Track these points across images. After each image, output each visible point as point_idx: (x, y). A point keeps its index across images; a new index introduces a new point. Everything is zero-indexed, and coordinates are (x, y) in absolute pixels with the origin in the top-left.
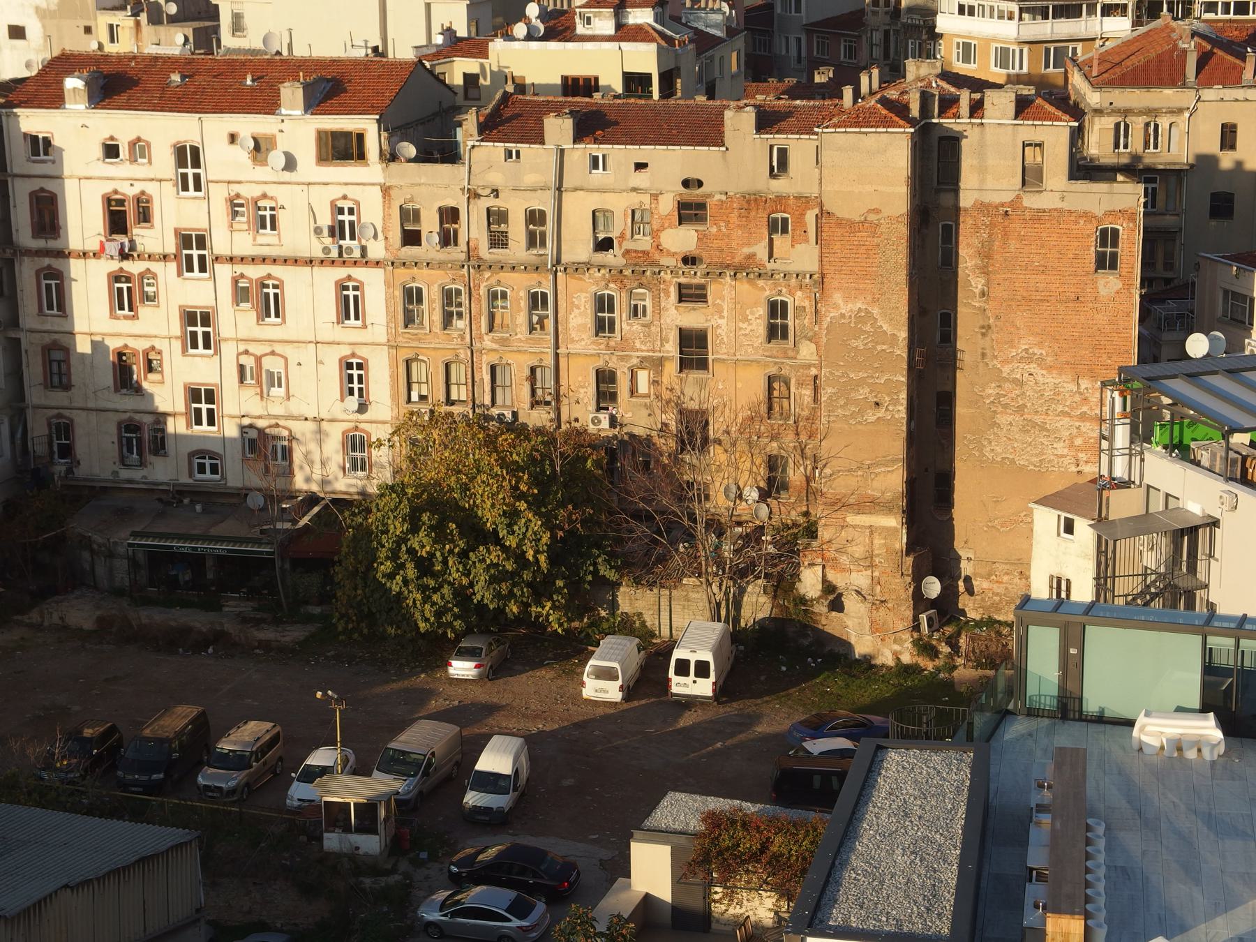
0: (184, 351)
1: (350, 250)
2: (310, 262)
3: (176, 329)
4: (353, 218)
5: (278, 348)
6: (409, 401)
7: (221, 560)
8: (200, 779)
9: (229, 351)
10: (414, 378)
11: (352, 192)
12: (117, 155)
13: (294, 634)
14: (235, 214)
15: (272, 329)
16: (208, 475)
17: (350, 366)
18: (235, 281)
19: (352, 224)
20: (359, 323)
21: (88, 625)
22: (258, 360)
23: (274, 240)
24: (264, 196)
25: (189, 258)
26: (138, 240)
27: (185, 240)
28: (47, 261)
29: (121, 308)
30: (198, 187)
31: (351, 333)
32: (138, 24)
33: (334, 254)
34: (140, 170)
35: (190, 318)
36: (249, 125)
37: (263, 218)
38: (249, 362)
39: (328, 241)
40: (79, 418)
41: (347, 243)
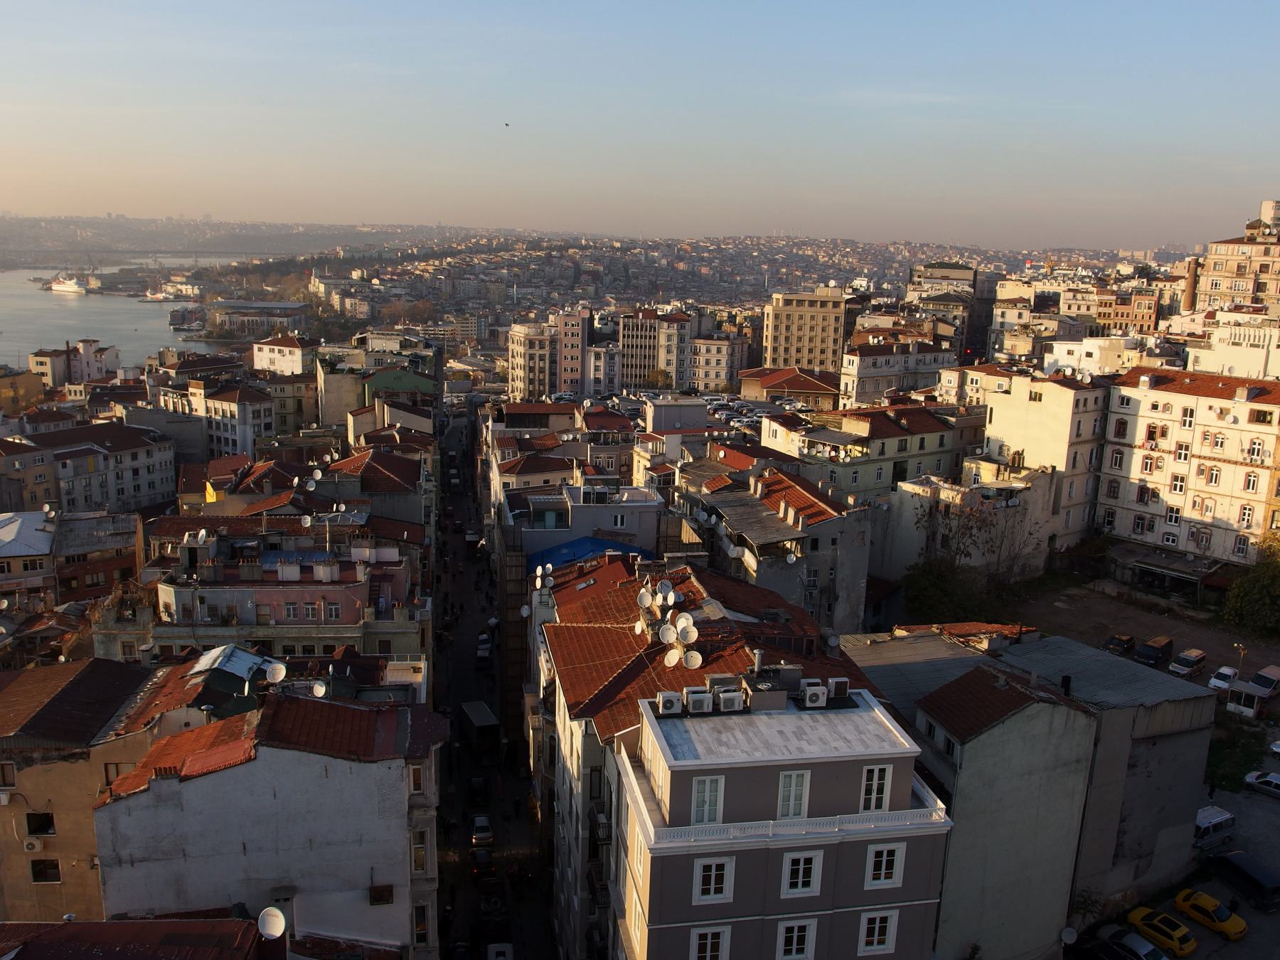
0: (1170, 491)
1: (1256, 460)
2: (1236, 463)
3: (1168, 482)
4: (1260, 447)
5: (1213, 496)
6: (1271, 528)
7: (1173, 578)
8: (1170, 667)
9: (1190, 494)
10: (1276, 519)
11: (1262, 436)
12: (1157, 409)
13: (1203, 616)
14: (1206, 439)
15: (1212, 488)
16: (1170, 543)
17: (1245, 509)
18: (1199, 466)
19: (1259, 450)
20: (1254, 491)
21: (1114, 594)
22: (1203, 500)
23: (1221, 452)
24: (1220, 433)
25: (1180, 454)
26: (1160, 444)
27: (1180, 447)
28: (1118, 447)
29: (1146, 470)
30: (1190, 426)
31: (1249, 495)
32: (1142, 356)
33: (1248, 461)
34: (1165, 416)
35: (1176, 478)
36: (1218, 403)
37: (1217, 442)
38: (1198, 500)
39: (1246, 455)
40: (1119, 511)
41: (1255, 457)
